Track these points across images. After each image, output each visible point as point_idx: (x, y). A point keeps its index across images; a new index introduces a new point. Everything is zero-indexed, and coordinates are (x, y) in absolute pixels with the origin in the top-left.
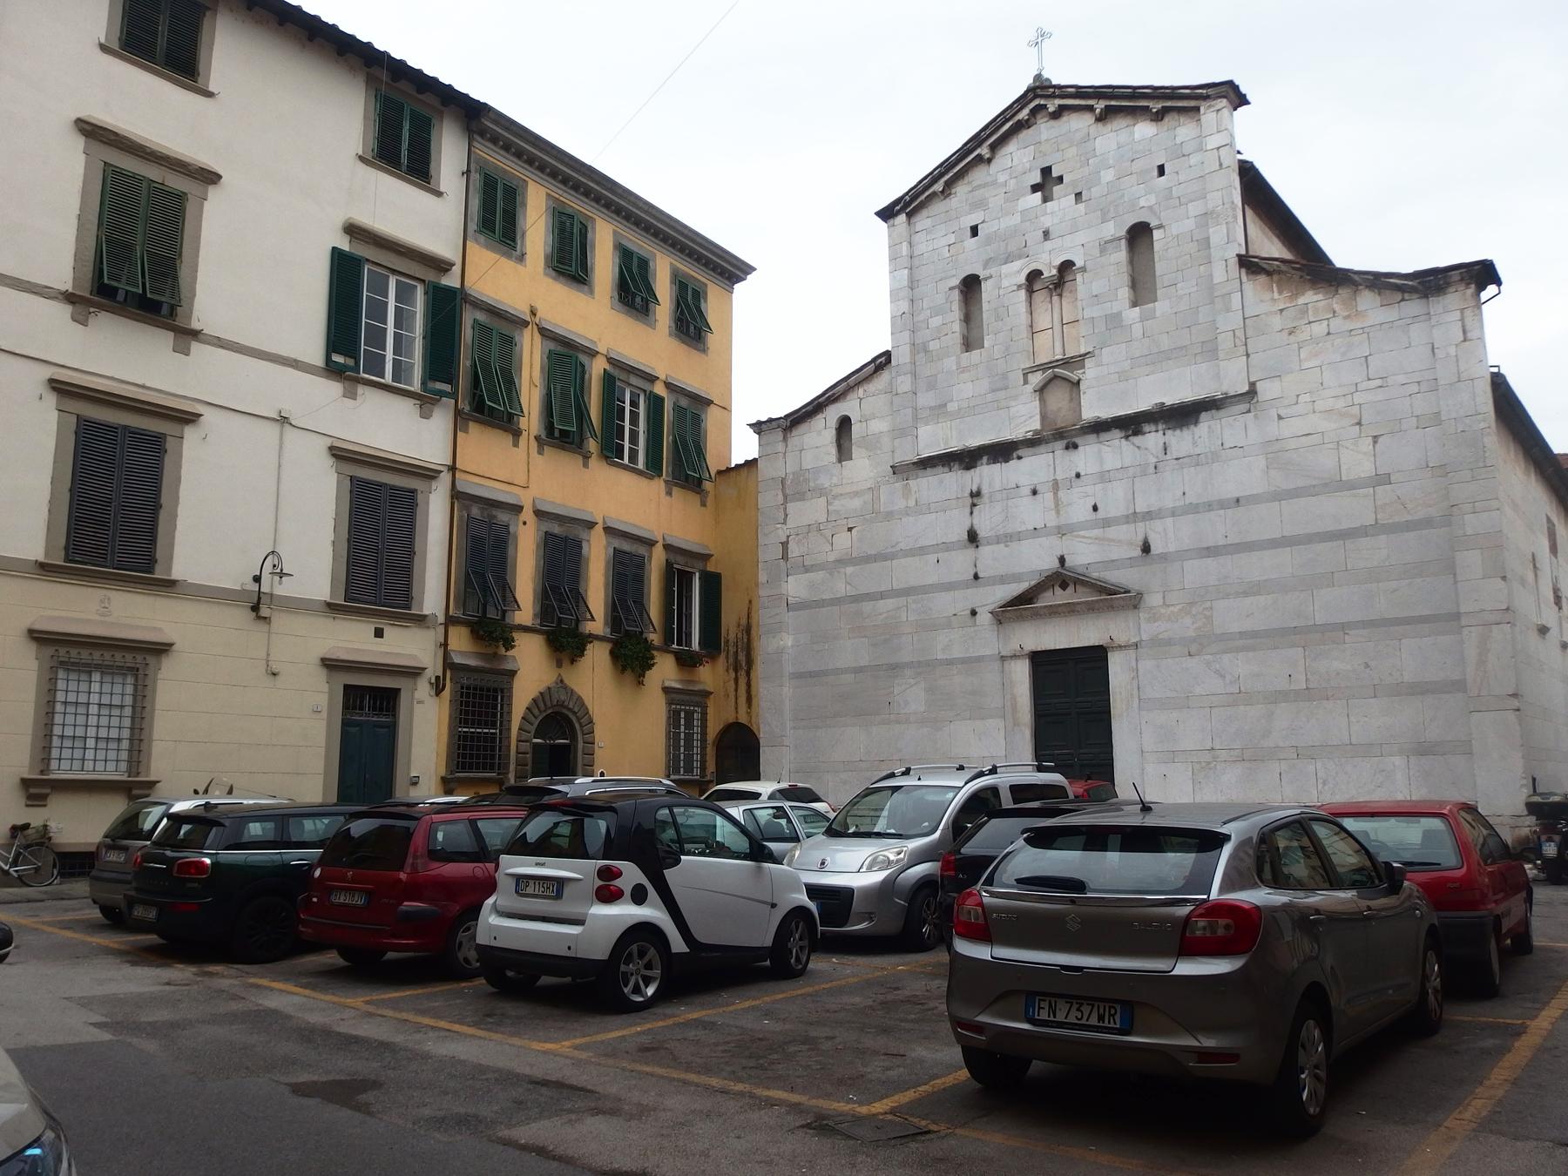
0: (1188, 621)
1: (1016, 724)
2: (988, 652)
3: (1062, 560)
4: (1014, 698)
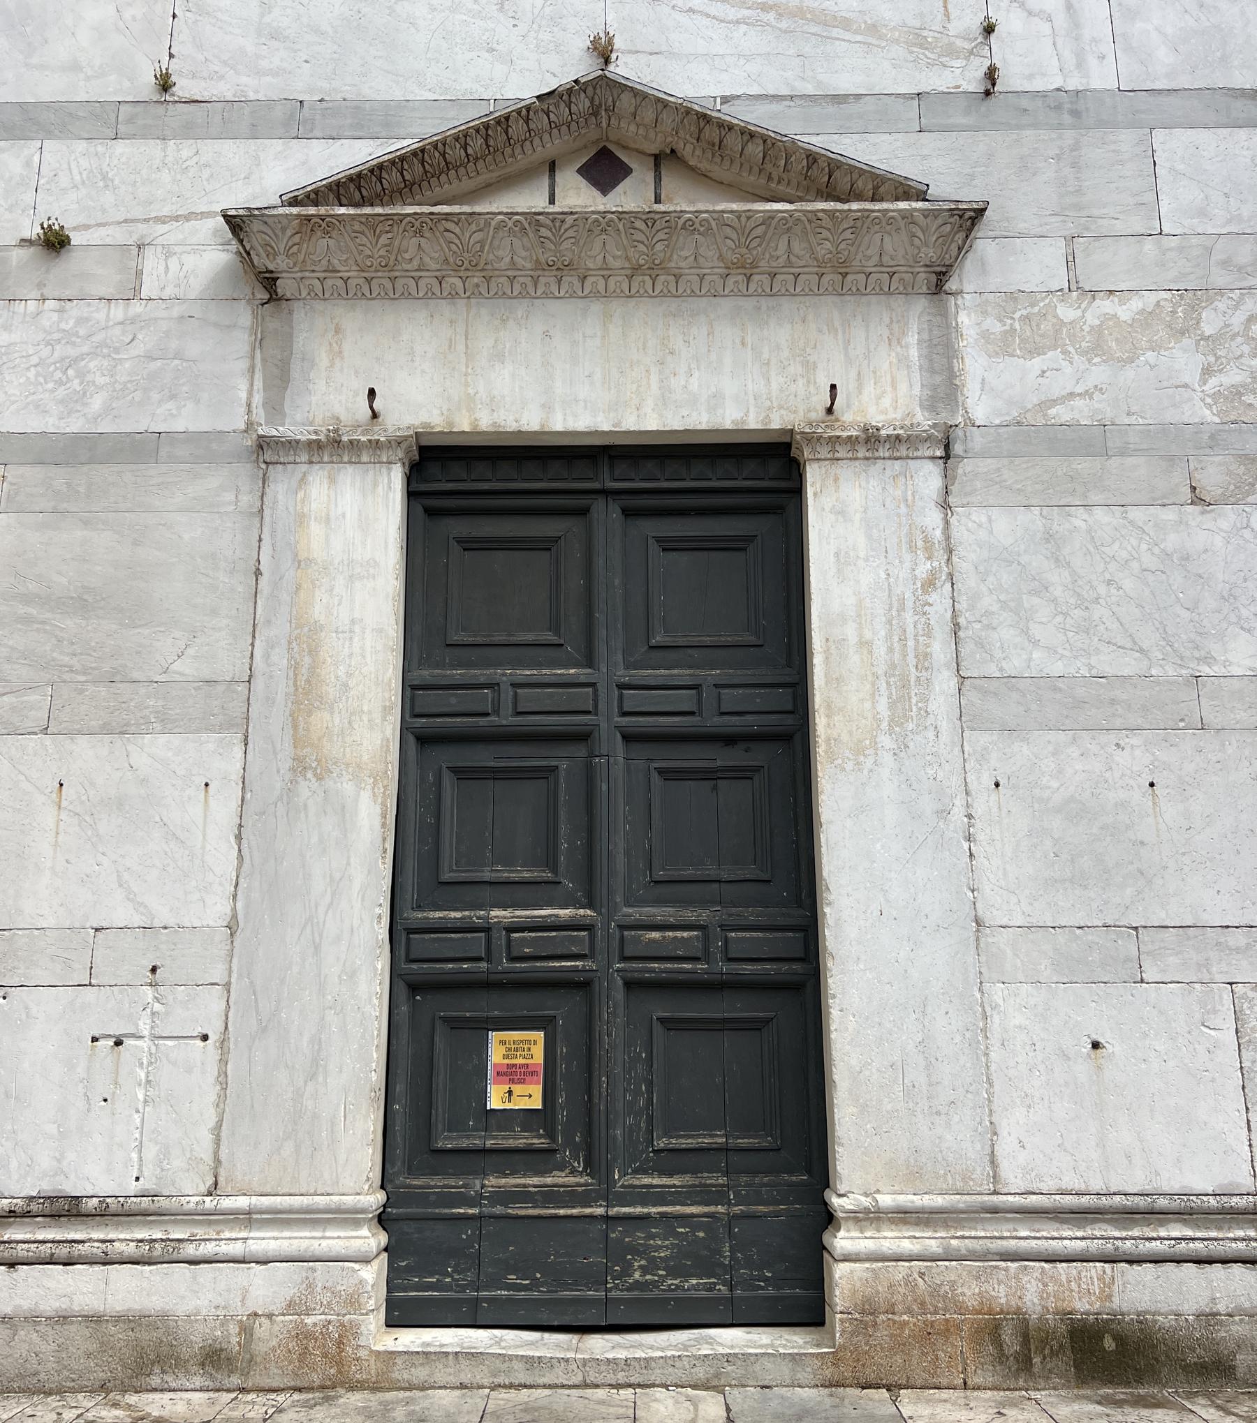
0: (1184, 361)
1: (307, 763)
2: (185, 418)
3: (603, 51)
4: (306, 642)
